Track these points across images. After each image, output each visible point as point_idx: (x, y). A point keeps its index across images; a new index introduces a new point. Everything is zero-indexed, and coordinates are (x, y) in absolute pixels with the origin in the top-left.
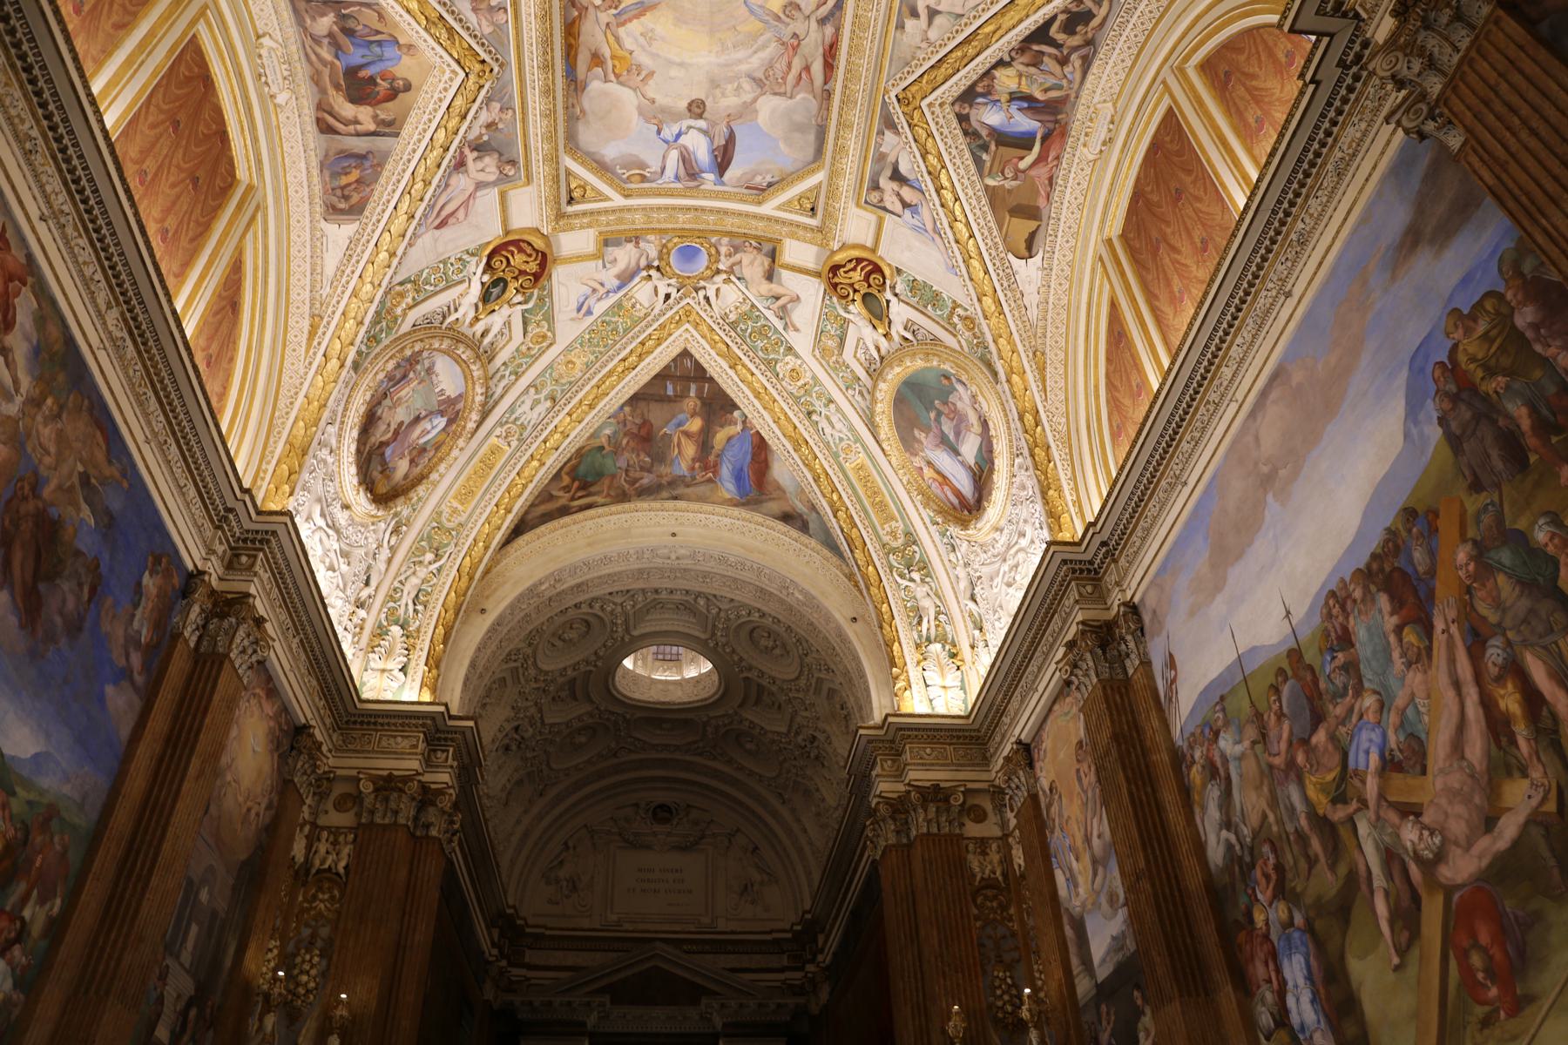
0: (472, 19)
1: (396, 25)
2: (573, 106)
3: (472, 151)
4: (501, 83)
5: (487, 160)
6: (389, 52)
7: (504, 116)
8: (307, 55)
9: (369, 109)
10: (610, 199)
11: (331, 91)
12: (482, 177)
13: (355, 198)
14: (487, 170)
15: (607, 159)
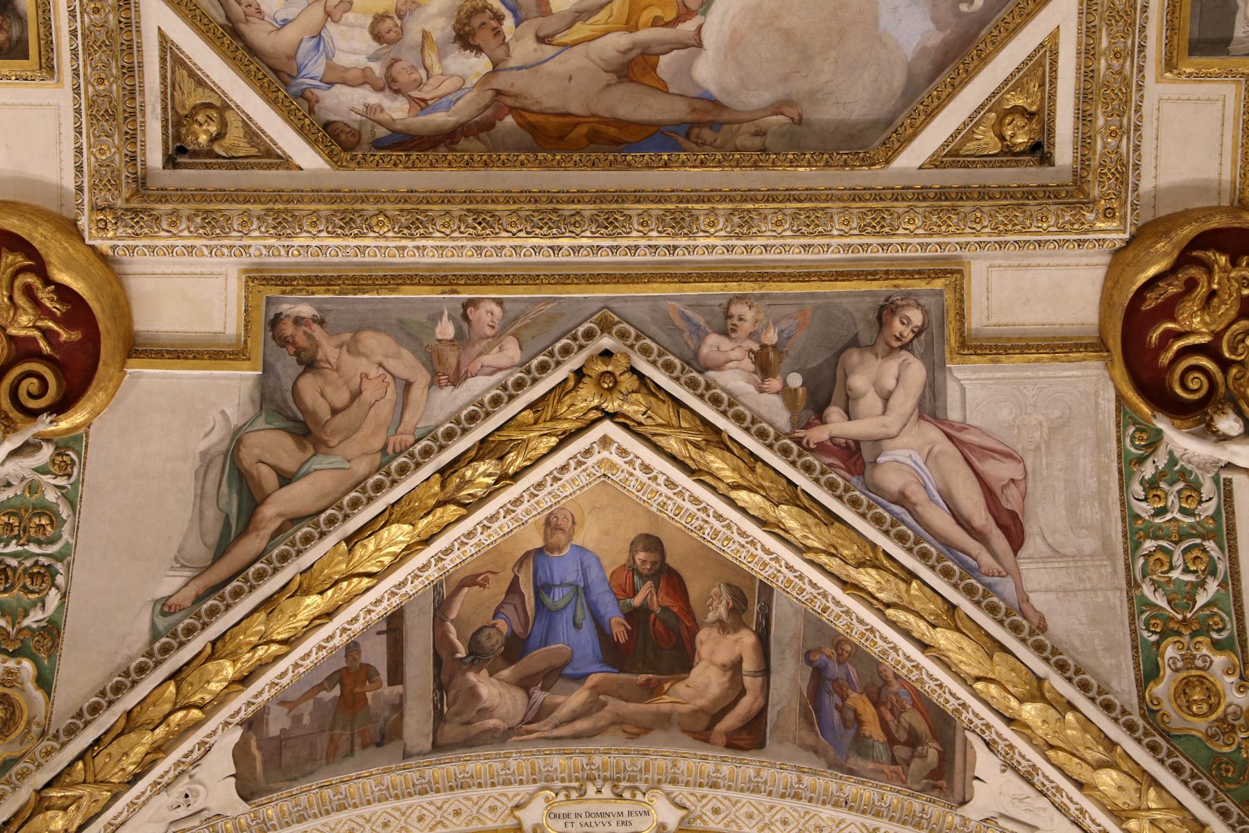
0: (478, 386)
1: (495, 551)
2: (761, 133)
3: (822, 420)
4: (653, 329)
5: (859, 381)
6: (564, 569)
7: (747, 327)
8: (576, 737)
9: (702, 635)
10: (1054, 35)
11: (663, 704)
12: (905, 402)
13: (912, 718)
14: (890, 383)
15: (936, 39)
